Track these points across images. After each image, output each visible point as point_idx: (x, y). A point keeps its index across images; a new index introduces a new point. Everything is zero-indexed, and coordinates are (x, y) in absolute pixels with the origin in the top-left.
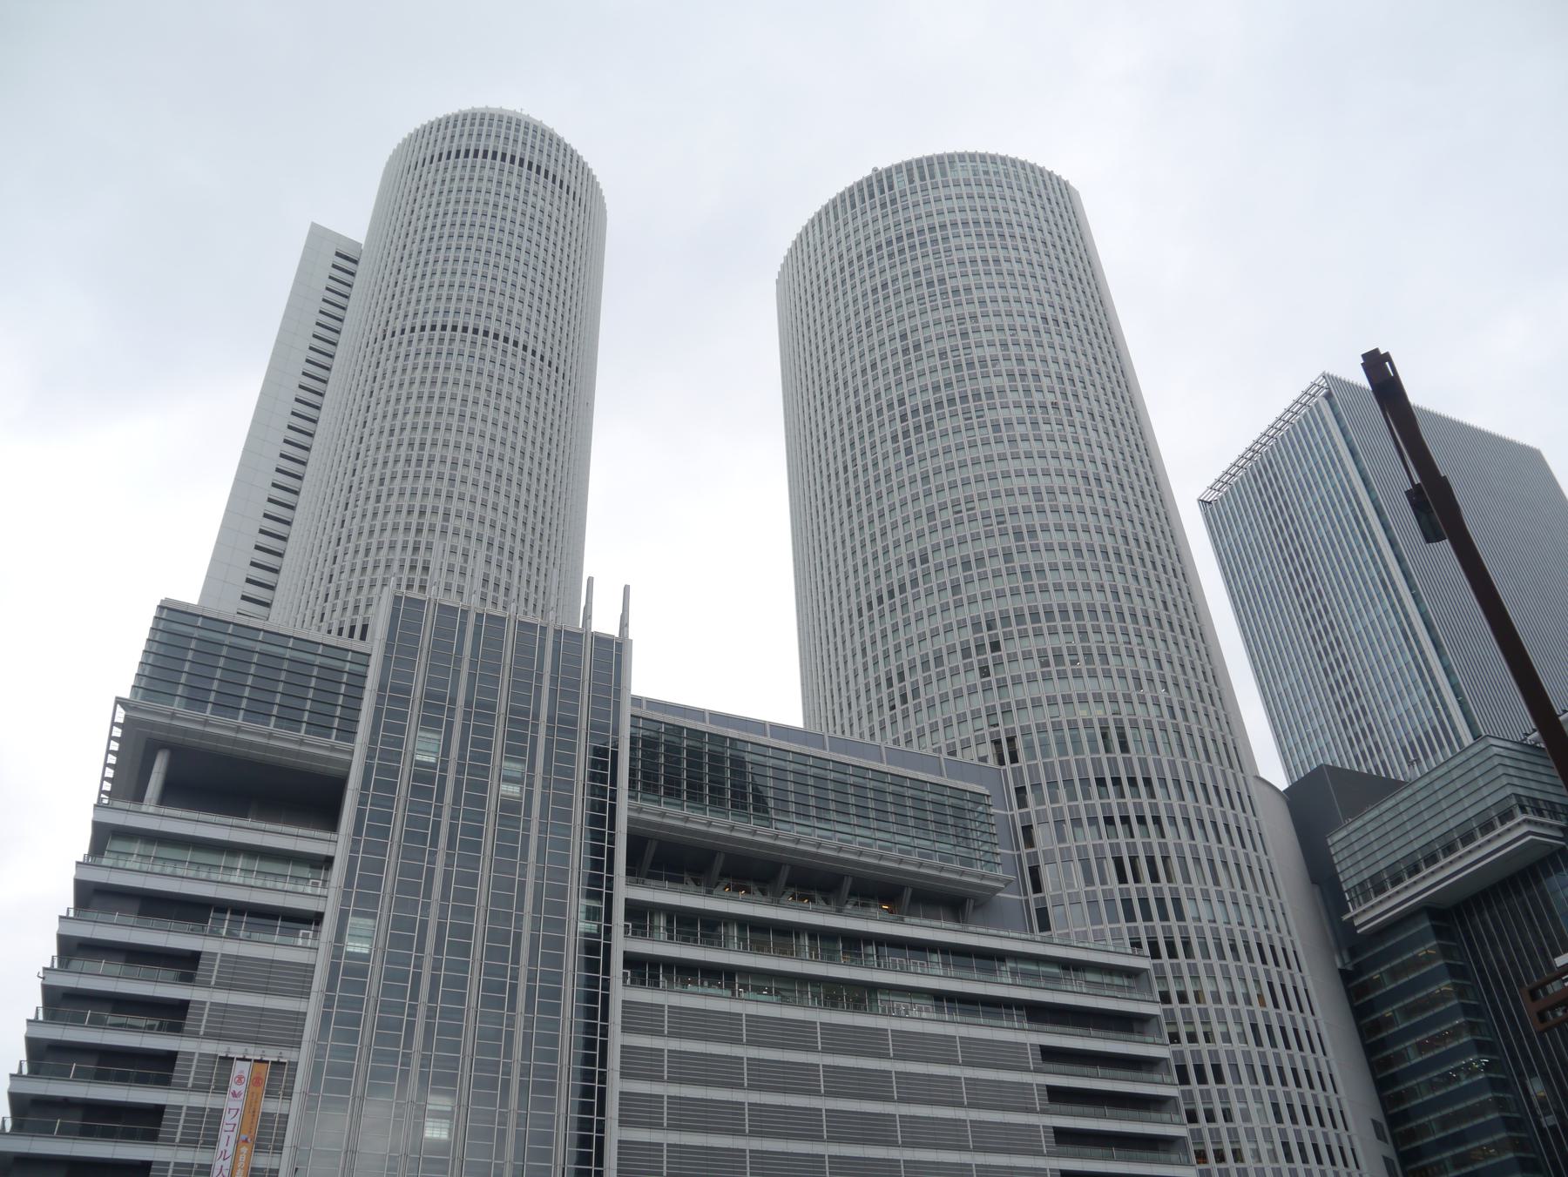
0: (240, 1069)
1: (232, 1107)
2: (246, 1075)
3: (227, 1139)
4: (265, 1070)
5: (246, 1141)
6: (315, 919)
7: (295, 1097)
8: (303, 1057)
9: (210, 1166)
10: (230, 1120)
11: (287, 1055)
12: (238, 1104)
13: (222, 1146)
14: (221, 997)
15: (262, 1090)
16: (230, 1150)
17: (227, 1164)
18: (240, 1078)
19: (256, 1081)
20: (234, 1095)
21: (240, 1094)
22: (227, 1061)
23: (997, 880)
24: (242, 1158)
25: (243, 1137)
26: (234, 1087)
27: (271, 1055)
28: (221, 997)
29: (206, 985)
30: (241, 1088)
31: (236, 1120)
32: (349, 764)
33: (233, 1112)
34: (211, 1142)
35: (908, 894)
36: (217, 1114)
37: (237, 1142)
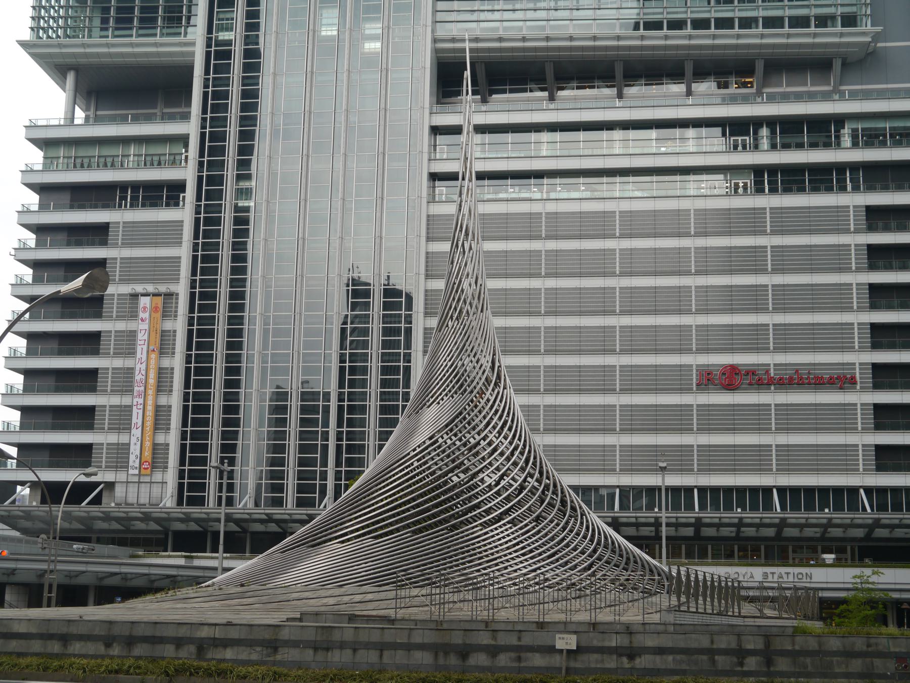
0: (145, 301)
1: (142, 328)
2: (148, 306)
3: (141, 350)
4: (159, 301)
5: (153, 350)
6: (180, 186)
7: (179, 317)
8: (182, 289)
9: (132, 369)
10: (142, 337)
11: (173, 288)
12: (144, 326)
13: (139, 355)
14: (127, 253)
15: (159, 315)
16: (144, 358)
17: (143, 366)
18: (145, 308)
19: (155, 309)
20: (142, 320)
21: (146, 318)
22: (135, 296)
23: (864, 34)
24: (153, 362)
25: (151, 348)
26: (142, 315)
27: (163, 288)
28: (127, 253)
29: (115, 245)
30: (146, 315)
31: (146, 337)
32: (193, 54)
33: (143, 332)
34: (131, 352)
35: (760, 66)
36: (133, 334)
37: (148, 352)
